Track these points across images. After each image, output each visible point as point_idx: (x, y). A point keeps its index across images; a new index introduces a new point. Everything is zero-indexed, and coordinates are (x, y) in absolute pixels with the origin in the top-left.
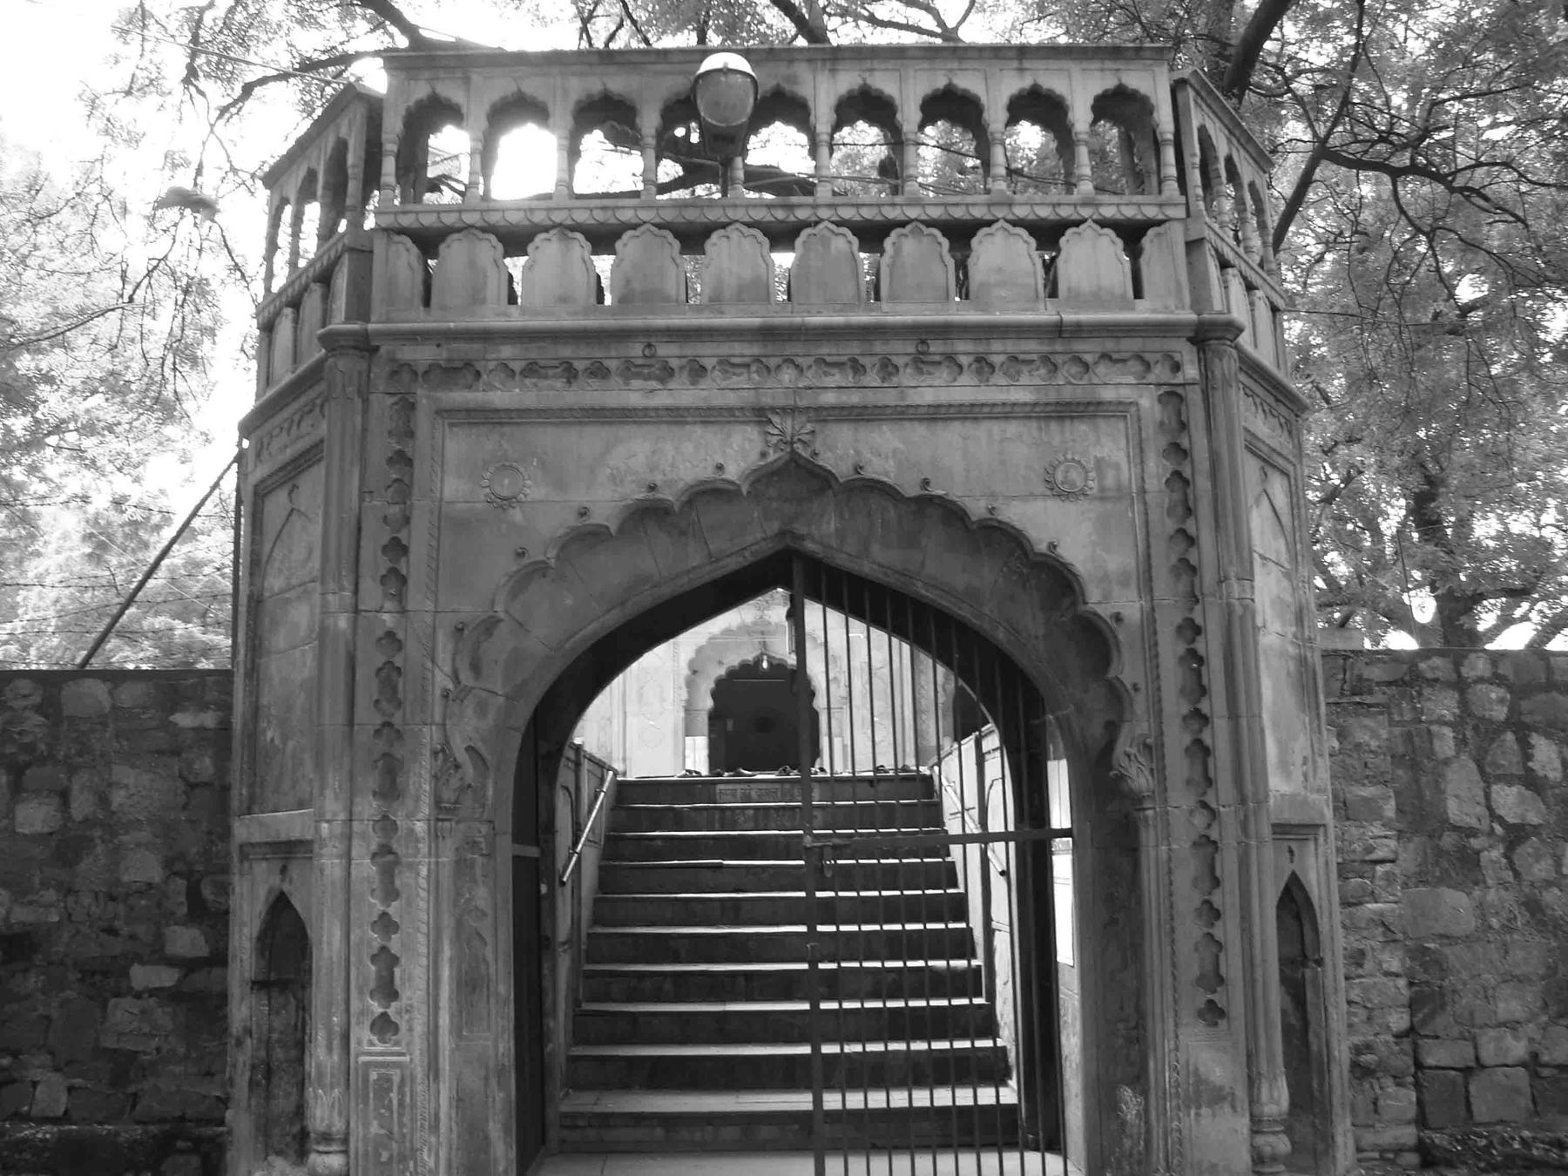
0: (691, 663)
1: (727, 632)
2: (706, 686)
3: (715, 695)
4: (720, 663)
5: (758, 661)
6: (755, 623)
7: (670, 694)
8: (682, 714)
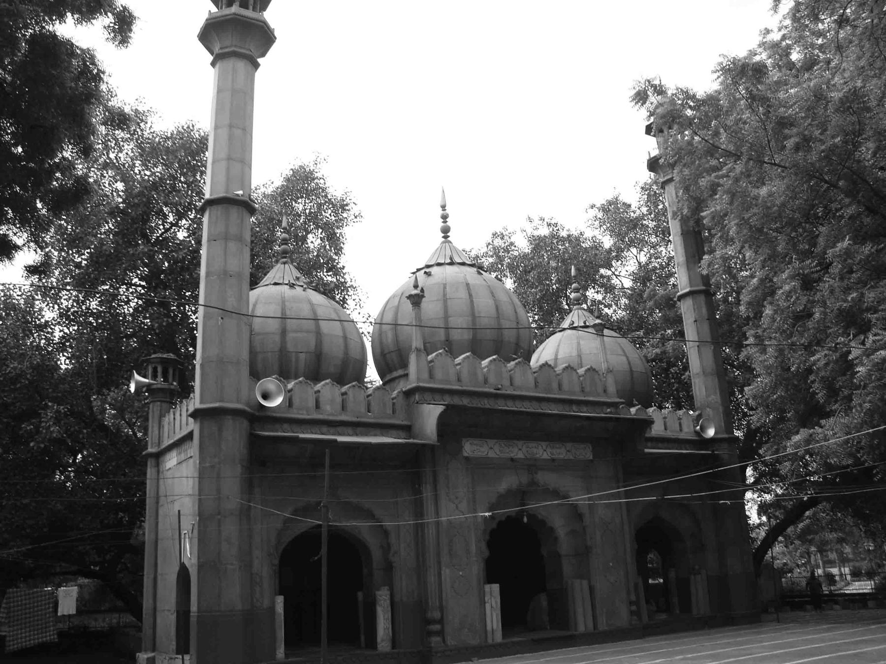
7: (473, 548)
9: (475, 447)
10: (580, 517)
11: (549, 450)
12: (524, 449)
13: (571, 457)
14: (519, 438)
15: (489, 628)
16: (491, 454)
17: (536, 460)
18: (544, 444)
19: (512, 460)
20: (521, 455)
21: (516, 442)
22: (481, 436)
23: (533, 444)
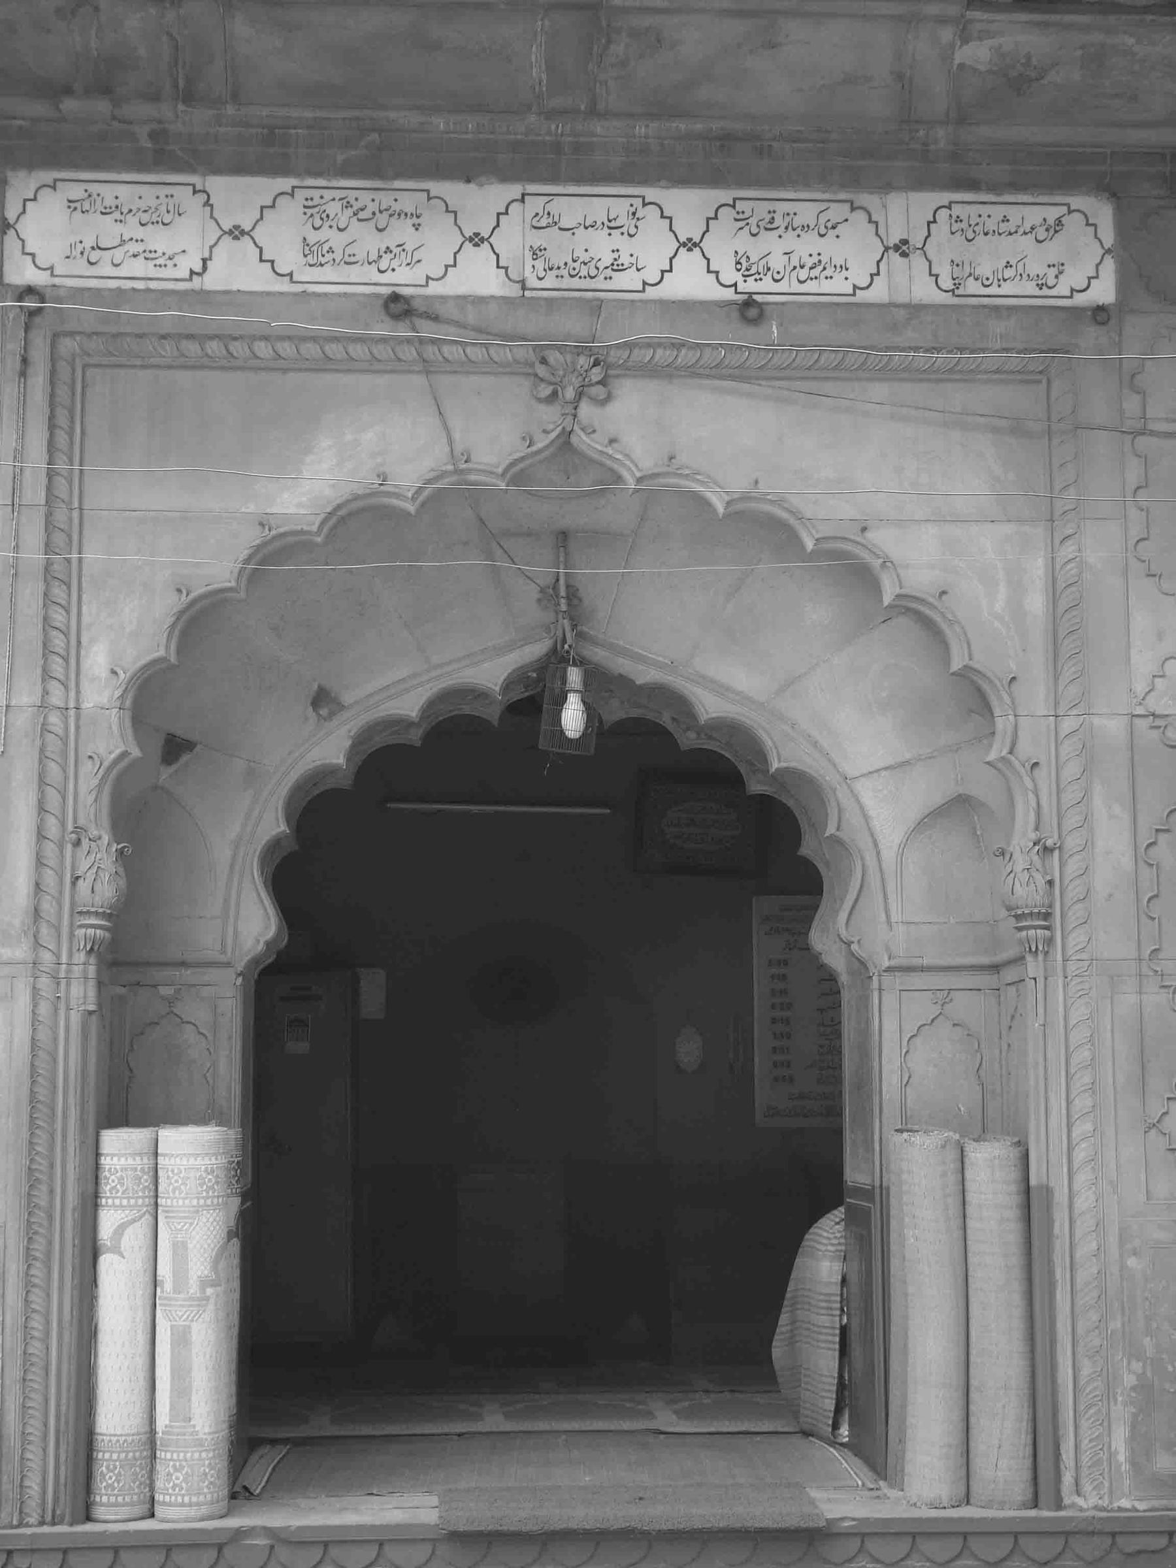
0: (147, 693)
1: (361, 521)
2: (237, 830)
3: (291, 876)
4: (323, 700)
5: (533, 701)
6: (518, 474)
8: (82, 994)
9: (109, 230)
10: (974, 698)
11: (723, 246)
12: (512, 239)
13: (924, 291)
14: (471, 165)
15: (116, 1415)
16: (235, 271)
17: (596, 307)
18: (688, 205)
19: (398, 306)
20: (478, 276)
21: (450, 190)
22: (164, 155)
23: (575, 206)
